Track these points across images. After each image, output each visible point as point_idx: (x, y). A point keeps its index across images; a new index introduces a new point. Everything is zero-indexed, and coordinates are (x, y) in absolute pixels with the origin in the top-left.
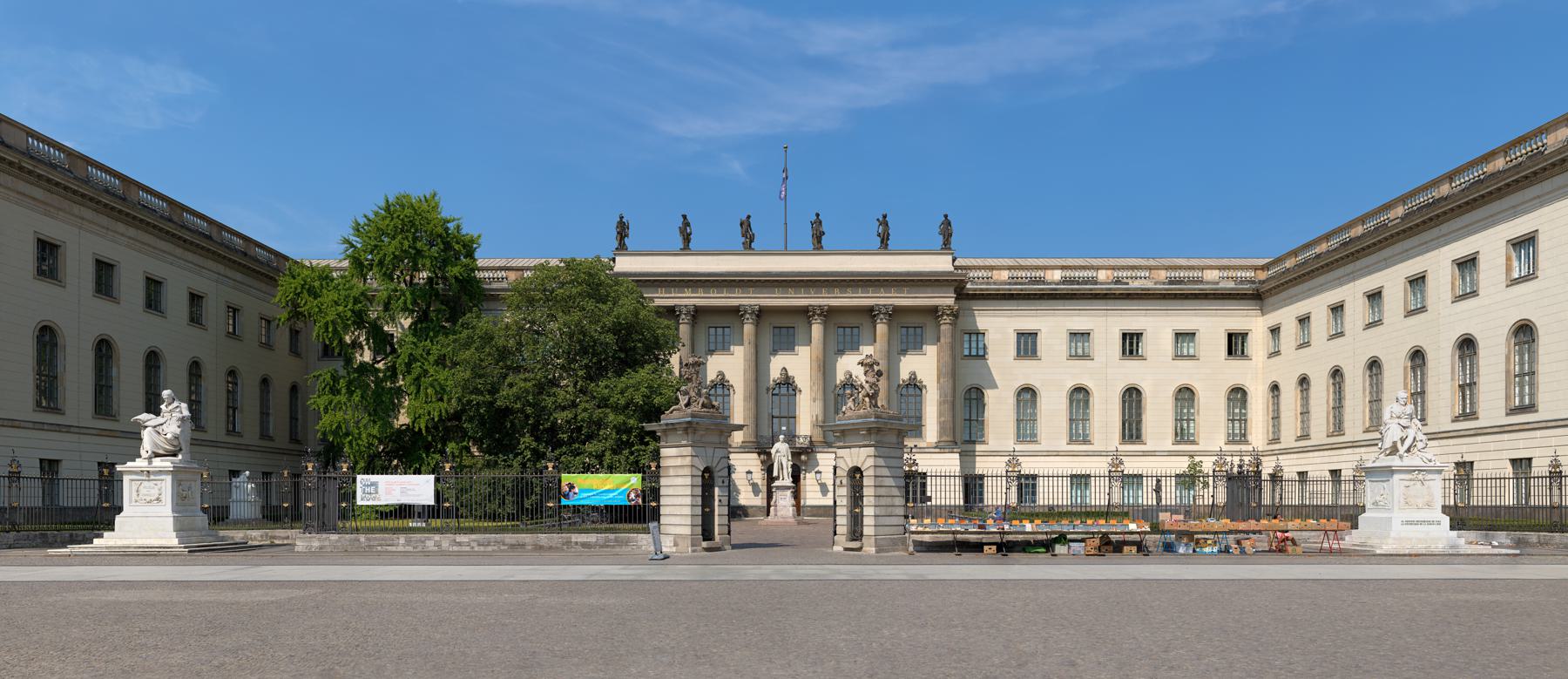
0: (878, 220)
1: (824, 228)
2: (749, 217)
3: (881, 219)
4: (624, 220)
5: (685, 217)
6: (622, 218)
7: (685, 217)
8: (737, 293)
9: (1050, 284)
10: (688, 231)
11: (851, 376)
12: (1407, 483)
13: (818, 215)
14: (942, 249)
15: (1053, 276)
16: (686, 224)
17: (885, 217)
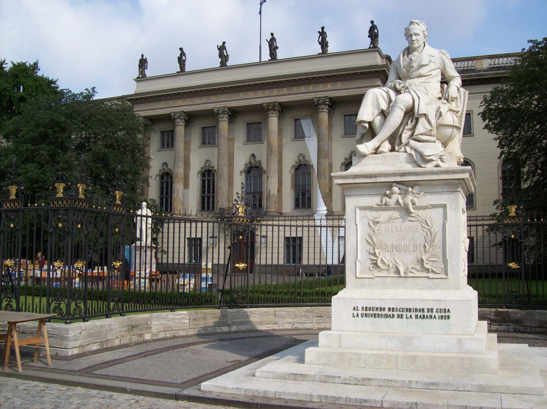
0: (319, 32)
1: (278, 43)
2: (224, 43)
3: (321, 31)
4: (144, 58)
5: (181, 49)
6: (142, 56)
7: (181, 49)
8: (213, 99)
9: (479, 71)
10: (184, 58)
11: (304, 157)
12: (372, 215)
13: (272, 34)
14: (370, 48)
15: (482, 64)
16: (183, 54)
17: (323, 28)
